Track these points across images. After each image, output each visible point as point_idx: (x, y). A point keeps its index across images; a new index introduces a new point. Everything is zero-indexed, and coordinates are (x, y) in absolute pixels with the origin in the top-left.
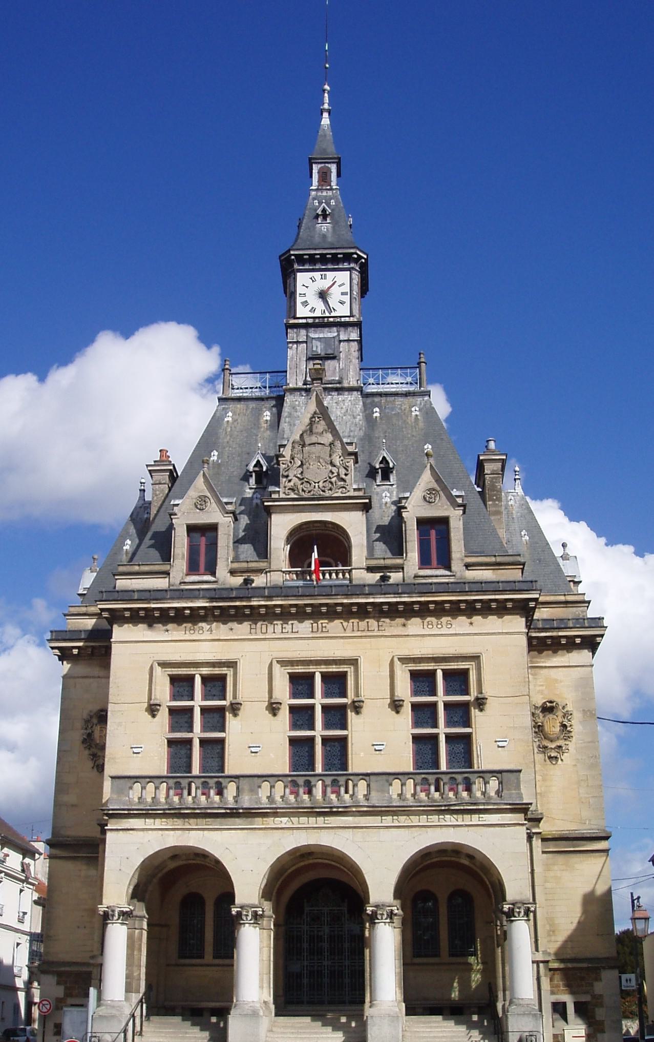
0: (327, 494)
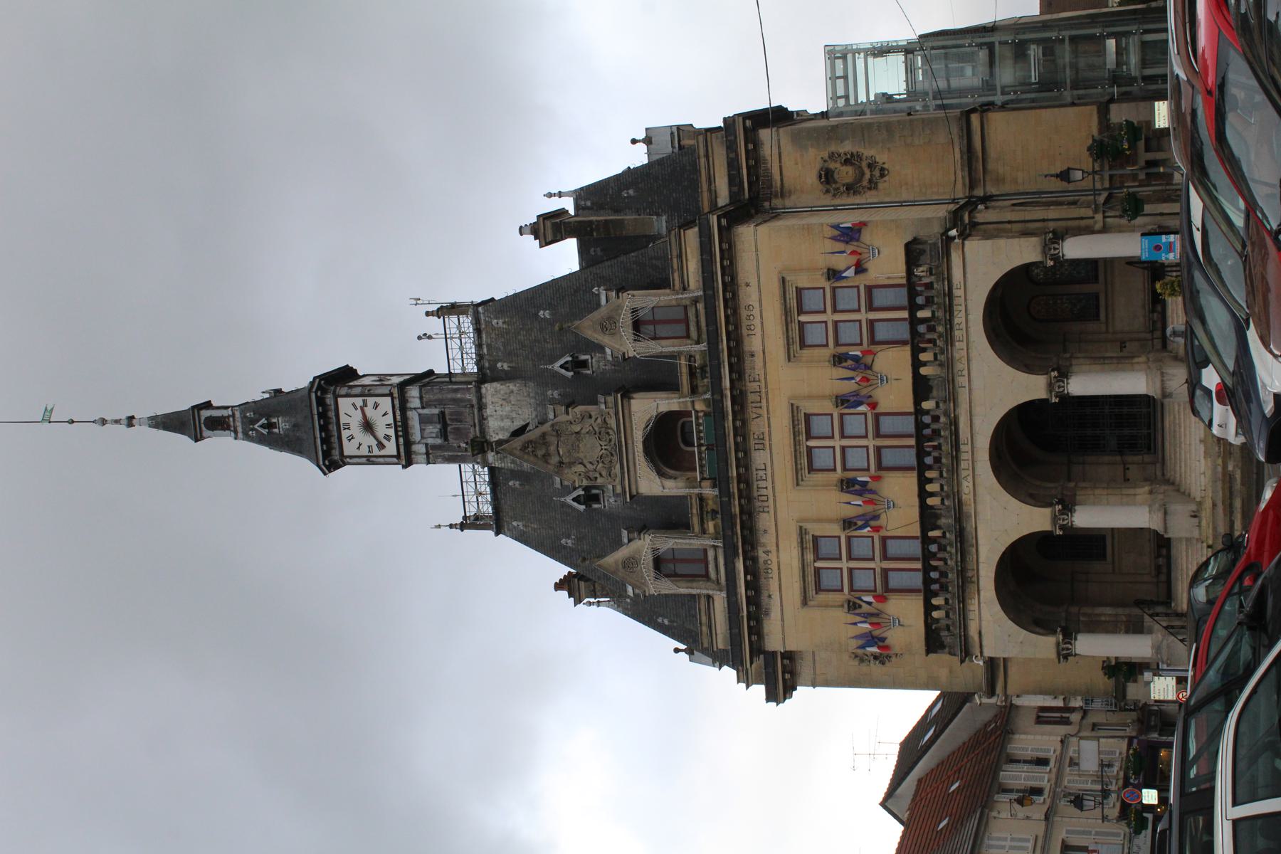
0: (613, 437)
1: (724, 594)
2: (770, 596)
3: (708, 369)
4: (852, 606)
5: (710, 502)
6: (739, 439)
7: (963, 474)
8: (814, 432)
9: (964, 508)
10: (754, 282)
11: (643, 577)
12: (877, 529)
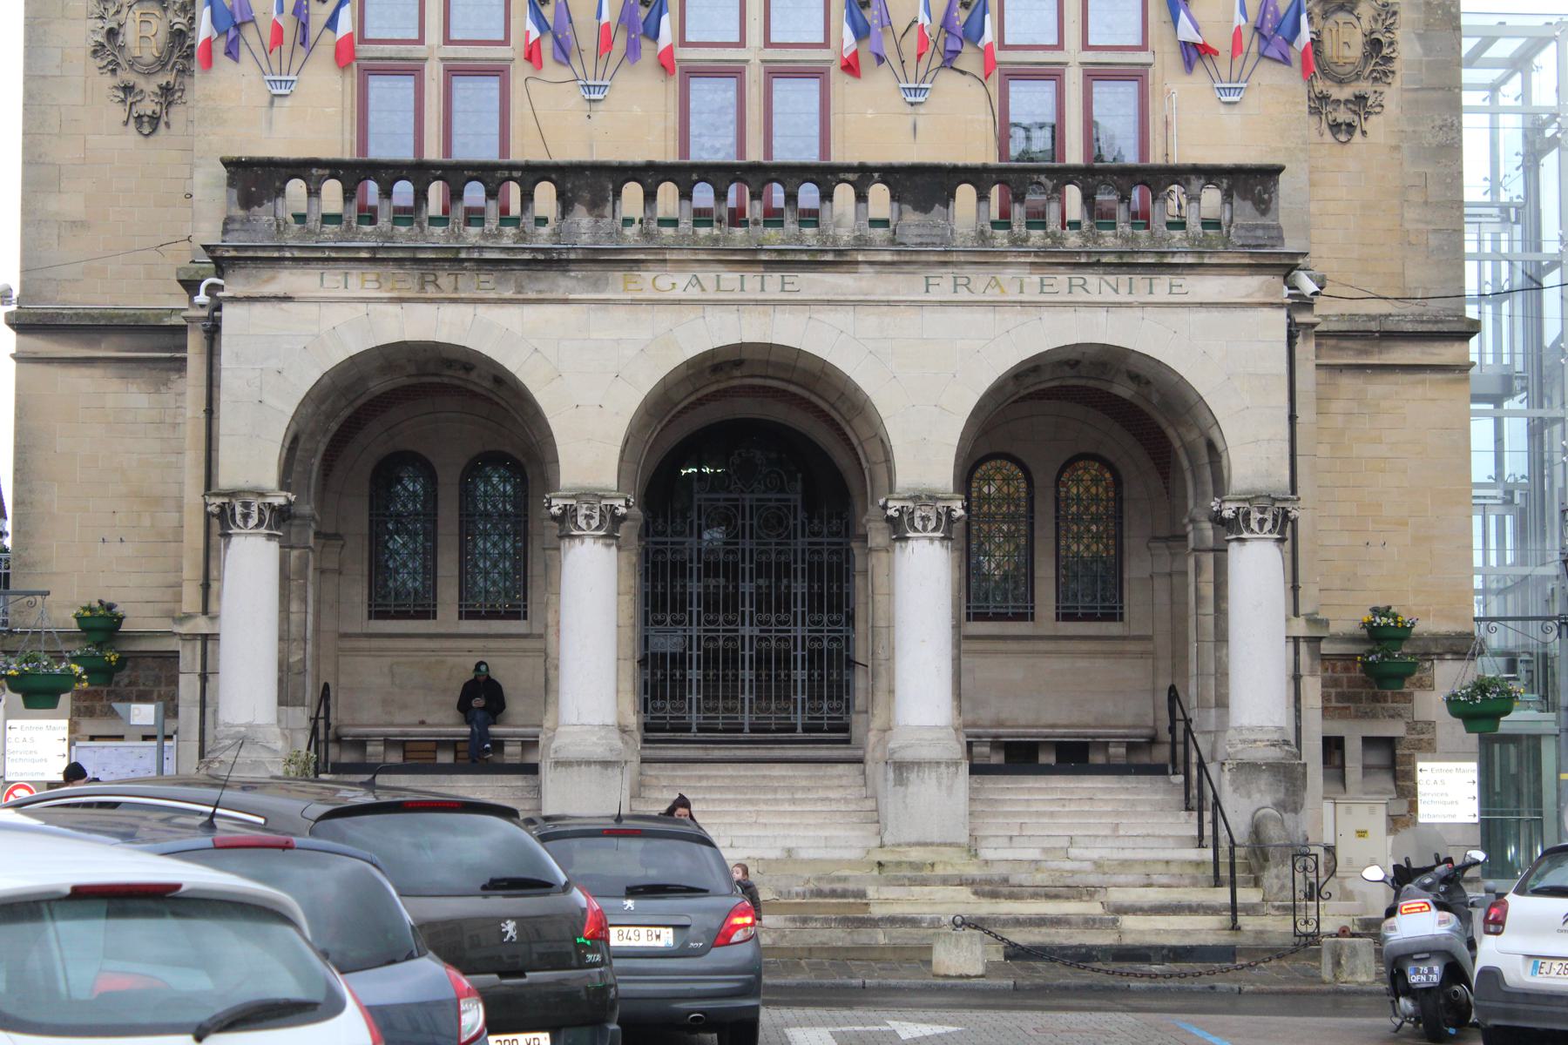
7: (708, 276)
9: (617, 276)
12: (532, 54)
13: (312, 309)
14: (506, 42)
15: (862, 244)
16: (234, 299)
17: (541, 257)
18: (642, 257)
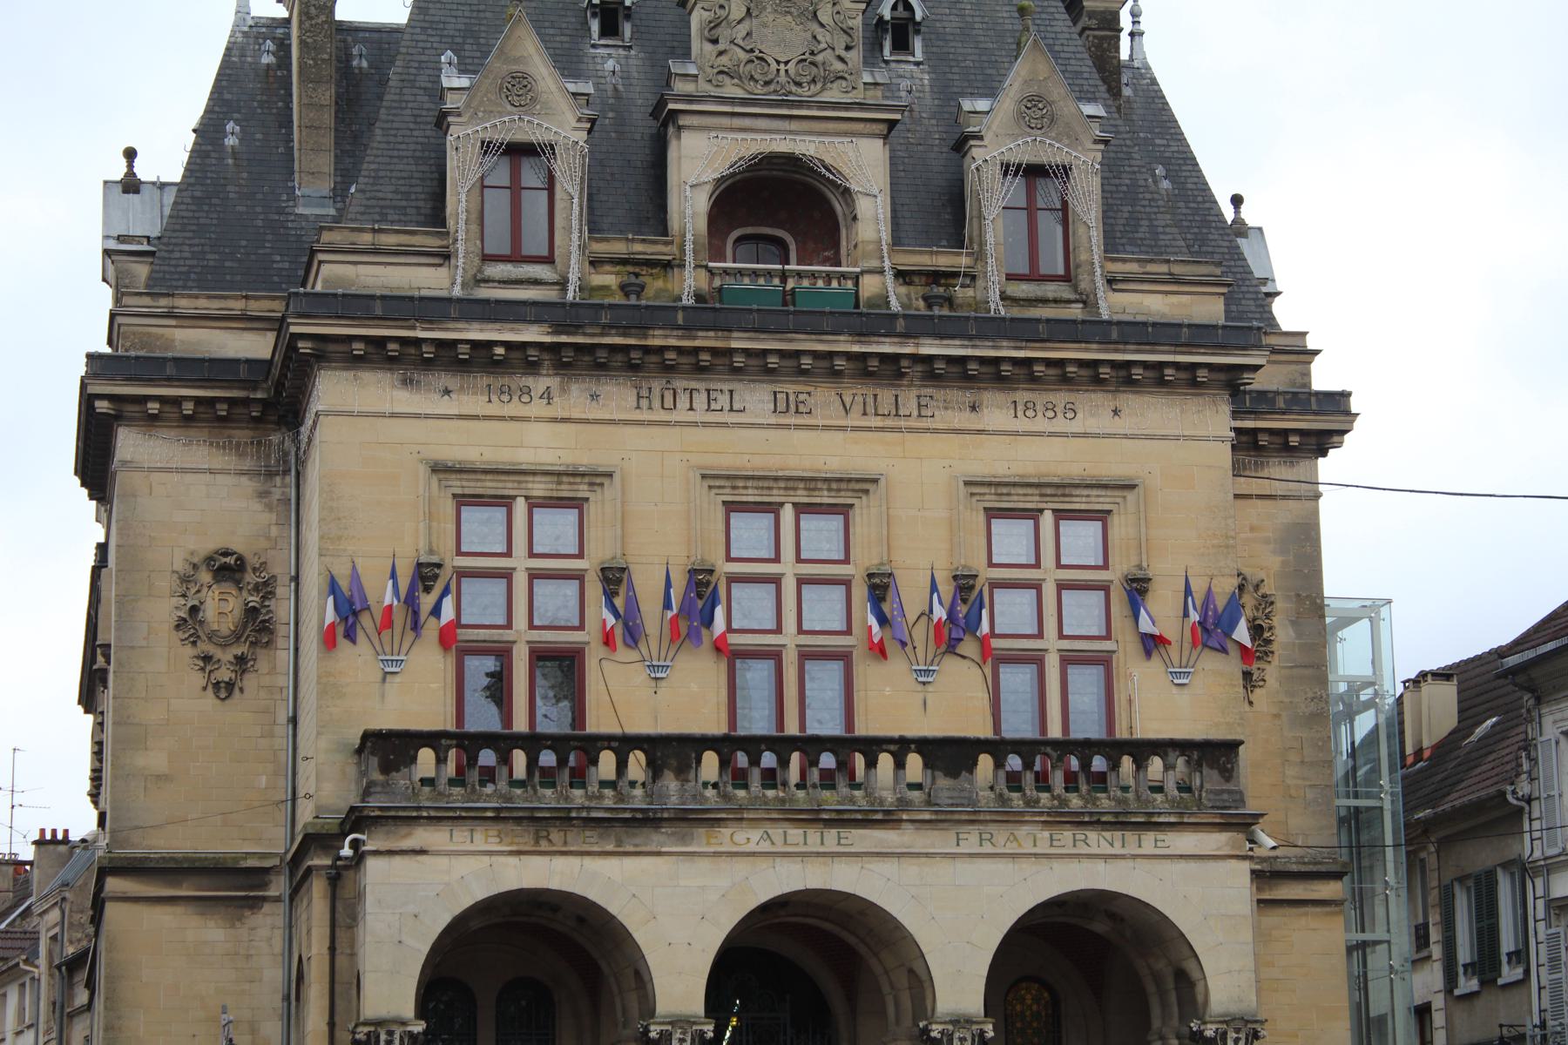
0: (805, 92)
1: (457, 292)
2: (447, 392)
3: (945, 312)
4: (425, 574)
5: (659, 284)
6: (806, 362)
7: (777, 832)
8: (808, 522)
9: (701, 831)
10: (1123, 425)
11: (490, 113)
12: (608, 640)
13: (443, 861)
14: (581, 627)
15: (904, 804)
16: (376, 853)
17: (639, 816)
18: (724, 816)
